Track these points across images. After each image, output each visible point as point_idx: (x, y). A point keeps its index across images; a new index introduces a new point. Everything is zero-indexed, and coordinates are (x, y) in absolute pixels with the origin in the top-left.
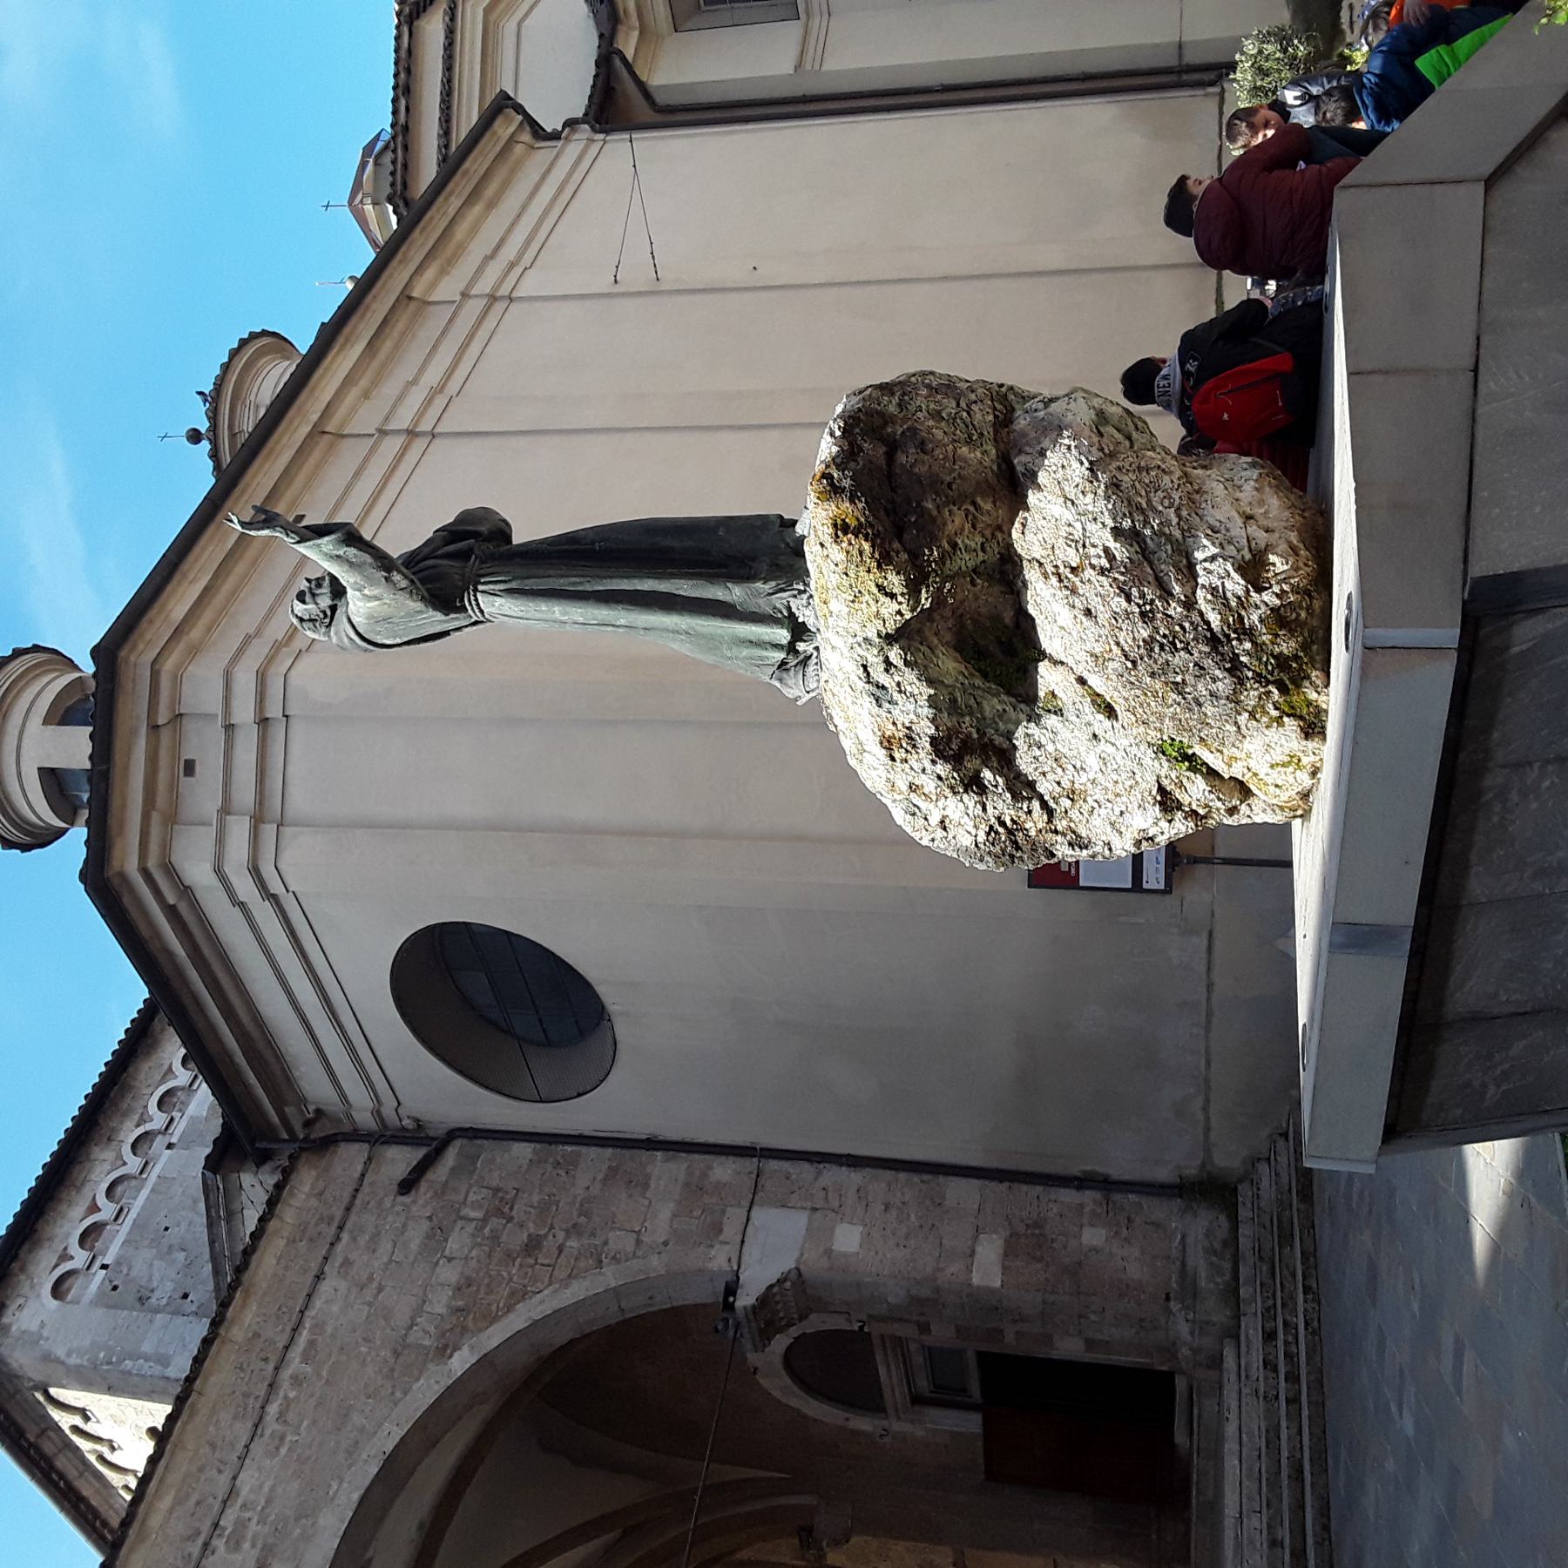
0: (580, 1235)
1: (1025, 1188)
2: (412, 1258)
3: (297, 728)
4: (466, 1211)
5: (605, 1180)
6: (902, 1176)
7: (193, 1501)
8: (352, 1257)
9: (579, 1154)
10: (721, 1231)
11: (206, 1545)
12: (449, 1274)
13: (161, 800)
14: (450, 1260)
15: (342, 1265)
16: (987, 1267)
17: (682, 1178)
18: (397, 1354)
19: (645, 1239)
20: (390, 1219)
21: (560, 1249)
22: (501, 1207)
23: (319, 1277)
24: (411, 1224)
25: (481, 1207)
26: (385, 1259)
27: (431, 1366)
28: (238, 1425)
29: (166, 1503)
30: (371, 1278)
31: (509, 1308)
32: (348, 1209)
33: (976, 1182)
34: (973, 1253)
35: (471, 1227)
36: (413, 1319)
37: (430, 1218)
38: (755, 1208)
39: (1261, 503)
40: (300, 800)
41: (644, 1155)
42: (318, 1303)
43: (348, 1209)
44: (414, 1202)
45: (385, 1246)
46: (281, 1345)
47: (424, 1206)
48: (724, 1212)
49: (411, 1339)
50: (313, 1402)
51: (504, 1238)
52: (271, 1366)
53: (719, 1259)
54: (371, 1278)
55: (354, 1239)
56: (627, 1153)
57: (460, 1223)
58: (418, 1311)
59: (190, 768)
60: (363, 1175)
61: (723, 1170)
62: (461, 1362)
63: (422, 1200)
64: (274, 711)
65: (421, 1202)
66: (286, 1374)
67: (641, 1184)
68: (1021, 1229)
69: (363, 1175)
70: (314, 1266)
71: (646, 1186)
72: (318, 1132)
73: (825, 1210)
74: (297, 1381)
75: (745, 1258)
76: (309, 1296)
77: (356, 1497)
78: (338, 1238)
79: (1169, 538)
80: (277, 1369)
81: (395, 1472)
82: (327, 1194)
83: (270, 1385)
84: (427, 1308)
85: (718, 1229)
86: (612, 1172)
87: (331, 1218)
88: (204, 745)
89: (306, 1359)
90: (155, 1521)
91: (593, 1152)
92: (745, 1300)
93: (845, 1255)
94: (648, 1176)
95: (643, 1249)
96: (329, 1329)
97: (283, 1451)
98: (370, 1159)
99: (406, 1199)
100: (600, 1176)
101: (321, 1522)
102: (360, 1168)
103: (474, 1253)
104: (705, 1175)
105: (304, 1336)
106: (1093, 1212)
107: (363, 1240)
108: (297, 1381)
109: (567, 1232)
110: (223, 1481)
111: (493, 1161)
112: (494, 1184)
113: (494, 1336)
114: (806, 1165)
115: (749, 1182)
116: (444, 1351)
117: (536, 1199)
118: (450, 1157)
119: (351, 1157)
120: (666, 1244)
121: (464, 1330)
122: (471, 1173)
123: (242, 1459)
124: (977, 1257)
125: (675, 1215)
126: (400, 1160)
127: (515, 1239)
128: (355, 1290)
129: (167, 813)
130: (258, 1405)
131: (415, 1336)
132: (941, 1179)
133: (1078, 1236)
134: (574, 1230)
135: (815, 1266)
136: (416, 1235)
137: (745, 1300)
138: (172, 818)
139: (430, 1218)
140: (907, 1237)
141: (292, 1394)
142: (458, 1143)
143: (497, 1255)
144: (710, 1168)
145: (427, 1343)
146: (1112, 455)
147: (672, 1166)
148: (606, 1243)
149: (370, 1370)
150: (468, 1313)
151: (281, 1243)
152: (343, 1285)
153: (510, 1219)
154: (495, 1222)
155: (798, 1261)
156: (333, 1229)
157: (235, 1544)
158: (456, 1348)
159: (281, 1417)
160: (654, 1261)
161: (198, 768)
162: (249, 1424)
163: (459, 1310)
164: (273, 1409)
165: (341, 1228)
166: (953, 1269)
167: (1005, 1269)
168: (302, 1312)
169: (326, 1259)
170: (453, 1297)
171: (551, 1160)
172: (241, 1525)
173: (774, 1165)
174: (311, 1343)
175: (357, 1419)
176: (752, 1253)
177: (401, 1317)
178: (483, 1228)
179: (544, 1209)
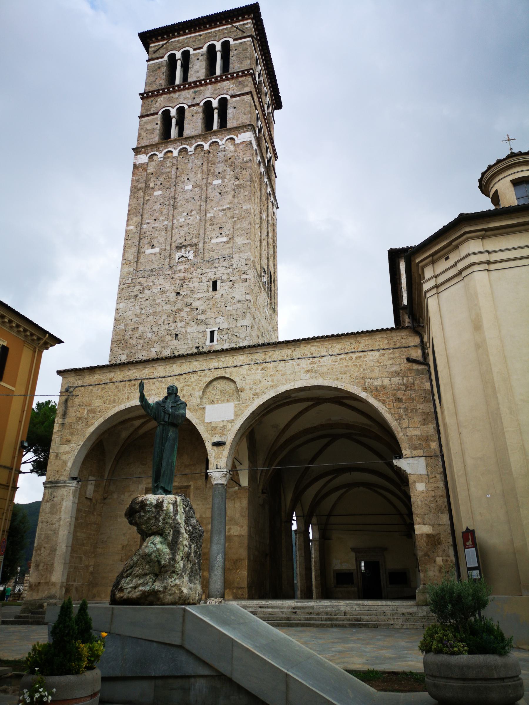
0: (405, 411)
1: (451, 538)
2: (389, 370)
3: (462, 283)
4: (405, 378)
5: (424, 412)
6: (446, 500)
7: (318, 349)
8: (386, 355)
9: (430, 402)
10: (414, 450)
11: (310, 357)
12: (386, 382)
13: (436, 257)
14: (390, 380)
15: (383, 354)
16: (421, 529)
17: (429, 434)
18: (362, 378)
19: (407, 430)
20: (399, 360)
21: (400, 408)
22: (408, 387)
23: (378, 350)
24: (398, 366)
25: (407, 382)
26: (387, 364)
27: (361, 388)
28: (337, 350)
29: (316, 344)
30: (381, 363)
31: (379, 401)
32: (399, 348)
33: (449, 522)
34: (424, 524)
35: (401, 382)
36: (372, 378)
37: (401, 370)
38: (424, 458)
39: (138, 591)
40: (444, 295)
41: (434, 421)
42: (371, 353)
43: (399, 348)
44: (405, 364)
45: (391, 362)
46: (359, 350)
47: (404, 367)
48: (421, 449)
49: (366, 380)
50: (346, 364)
51: (399, 392)
52: (353, 350)
53: (406, 452)
54: (381, 363)
55: (391, 353)
56: (434, 416)
57: (401, 378)
58: (374, 379)
59: (447, 259)
60: (410, 347)
61: (434, 445)
62: (363, 395)
63: (407, 365)
64: (464, 274)
65: (405, 365)
66: (351, 355)
67: (424, 422)
68: (436, 538)
69: (410, 347)
70: (382, 347)
71: (424, 425)
72: (419, 329)
73: (428, 478)
74: (351, 358)
75: (407, 459)
76: (373, 350)
77: (327, 385)
78: (390, 349)
79: (132, 572)
80: (352, 352)
81: (336, 389)
82: (402, 340)
83: (348, 353)
84: (376, 380)
85: (415, 448)
86: (427, 414)
87: (395, 345)
88: (454, 258)
89: (356, 358)
90: (312, 344)
91: (432, 406)
92: (396, 462)
93: (415, 487)
94: (427, 424)
95: (407, 430)
96: (365, 359)
97: (334, 363)
98: (415, 346)
99: (405, 360)
100: (424, 411)
101: (320, 379)
102: (413, 344)
103: (393, 386)
104: (432, 440)
105: (361, 354)
106: (447, 561)
107: (391, 356)
108: (351, 358)
109: (405, 408)
110: (323, 354)
111: (422, 379)
112: (416, 383)
113: (372, 401)
114: (442, 470)
115: (432, 454)
116: (365, 389)
117: (414, 396)
118: (421, 367)
119: (416, 340)
120: (407, 436)
121: (372, 392)
122: (418, 375)
123: (330, 355)
124: (424, 526)
125: (416, 435)
126: (417, 354)
127: (400, 394)
128: (376, 360)
129: (434, 260)
130: (343, 352)
131: (366, 380)
132: (447, 512)
133: (438, 556)
134: (406, 409)
135: (411, 479)
136: (397, 368)
137: (396, 462)
138: (433, 262)
139: (401, 370)
140: (426, 504)
141: (347, 359)
142: (426, 367)
143: (394, 392)
144: (434, 441)
145: (366, 384)
146: (143, 559)
147: (433, 430)
148: (404, 419)
149: (356, 374)
150: (375, 391)
151: (386, 336)
152: (377, 357)
153: (405, 391)
154: (403, 387)
155: (410, 474)
156: (392, 346)
157: (312, 363)
158: (366, 392)
159: (341, 359)
160: (401, 434)
161: (448, 261)
162: (338, 353)
163: (376, 388)
164: (343, 356)
165: (393, 349)
166: (418, 519)
167: (422, 535)
168: (368, 351)
169: (384, 349)
170: (379, 386)
171: (427, 395)
172: (316, 362)
173: (440, 460)
174: (361, 357)
175: (344, 376)
176: (410, 461)
177: (371, 375)
178: (401, 385)
179: (411, 399)
